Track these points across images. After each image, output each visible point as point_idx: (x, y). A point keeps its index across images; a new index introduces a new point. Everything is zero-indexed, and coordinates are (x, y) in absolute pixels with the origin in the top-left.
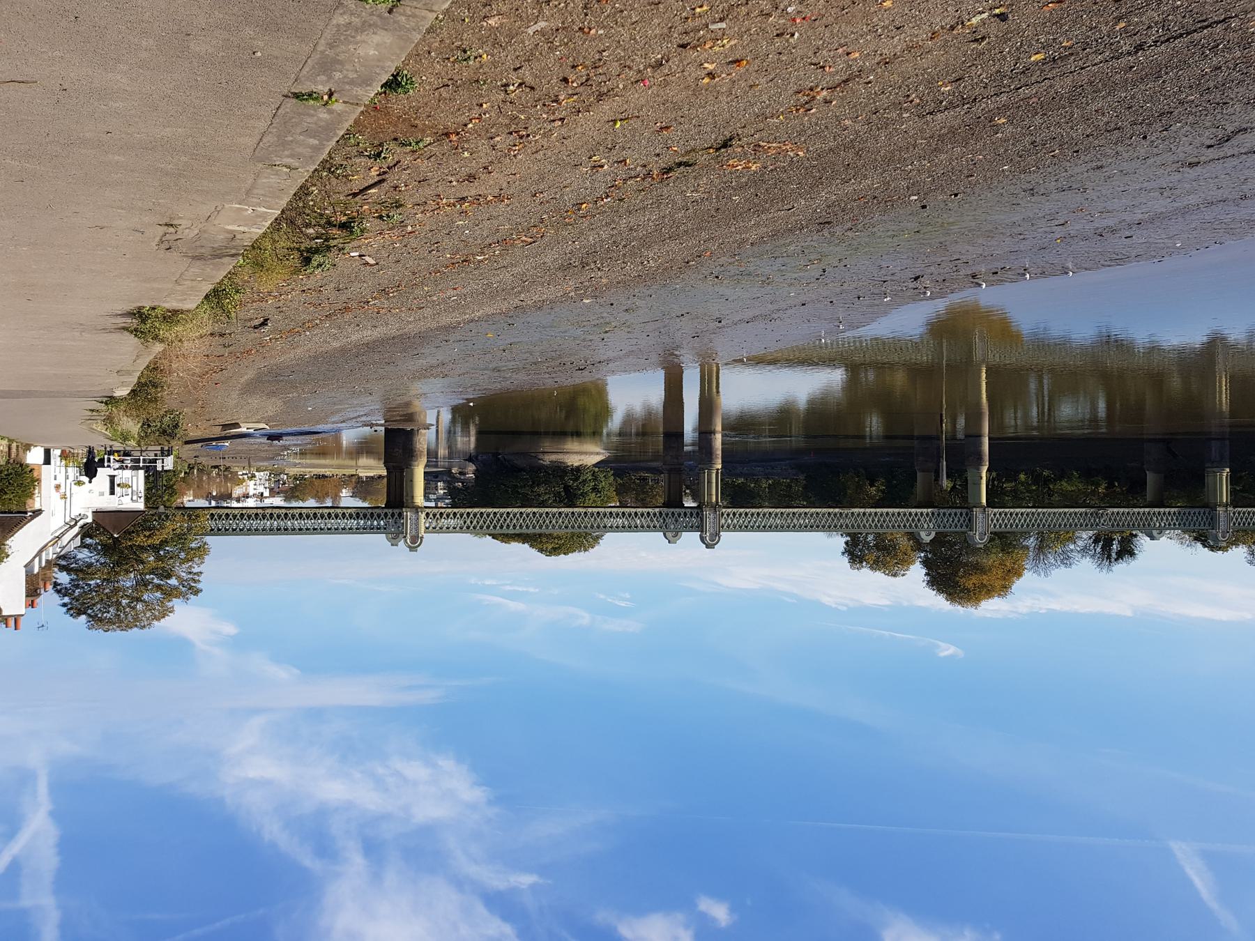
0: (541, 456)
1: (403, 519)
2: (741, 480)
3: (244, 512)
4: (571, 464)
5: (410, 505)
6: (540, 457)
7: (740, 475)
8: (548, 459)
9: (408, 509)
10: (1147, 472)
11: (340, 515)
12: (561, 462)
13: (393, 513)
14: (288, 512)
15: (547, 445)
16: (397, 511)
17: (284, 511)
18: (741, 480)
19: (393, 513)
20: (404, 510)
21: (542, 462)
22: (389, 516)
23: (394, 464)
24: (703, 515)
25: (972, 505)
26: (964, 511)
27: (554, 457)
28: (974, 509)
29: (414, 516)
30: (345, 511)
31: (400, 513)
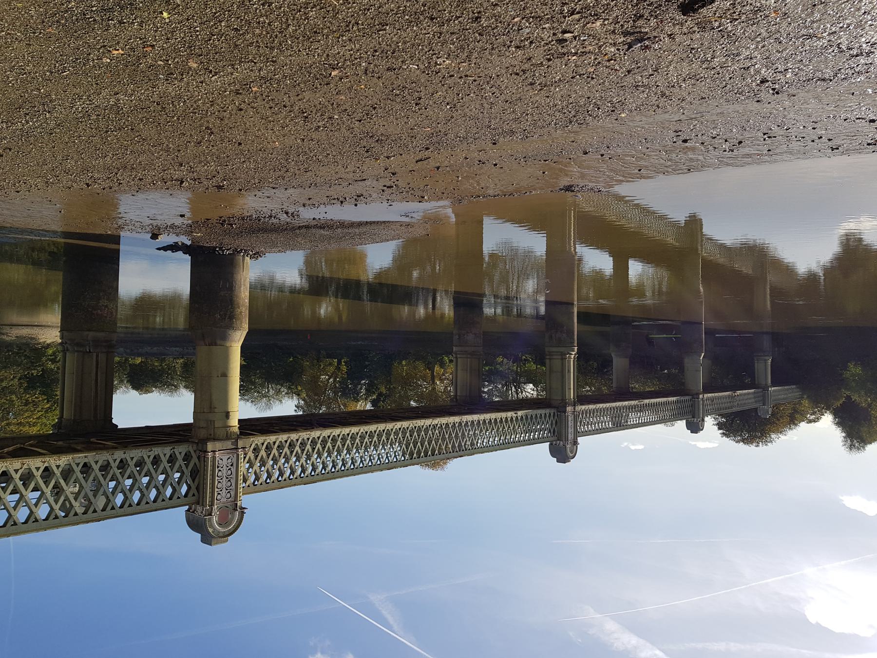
0: (6, 330)
2: (138, 360)
4: (44, 340)
5: (221, 433)
6: (5, 331)
7: (139, 355)
8: (13, 334)
9: (218, 445)
11: (37, 474)
12: (32, 339)
15: (15, 318)
18: (138, 360)
21: (4, 337)
22: (165, 463)
23: (101, 335)
27: (25, 332)
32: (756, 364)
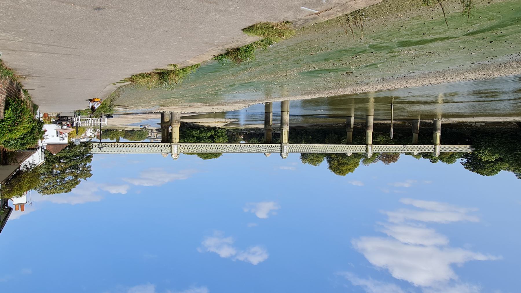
1: (171, 147)
3: (106, 144)
5: (174, 142)
9: (173, 144)
10: (413, 133)
13: (167, 145)
14: (124, 144)
16: (169, 144)
17: (123, 144)
19: (167, 145)
20: (172, 144)
24: (282, 146)
25: (367, 144)
26: (365, 145)
28: (368, 145)
29: (176, 146)
30: (148, 144)
31: (170, 145)
32: (433, 136)
